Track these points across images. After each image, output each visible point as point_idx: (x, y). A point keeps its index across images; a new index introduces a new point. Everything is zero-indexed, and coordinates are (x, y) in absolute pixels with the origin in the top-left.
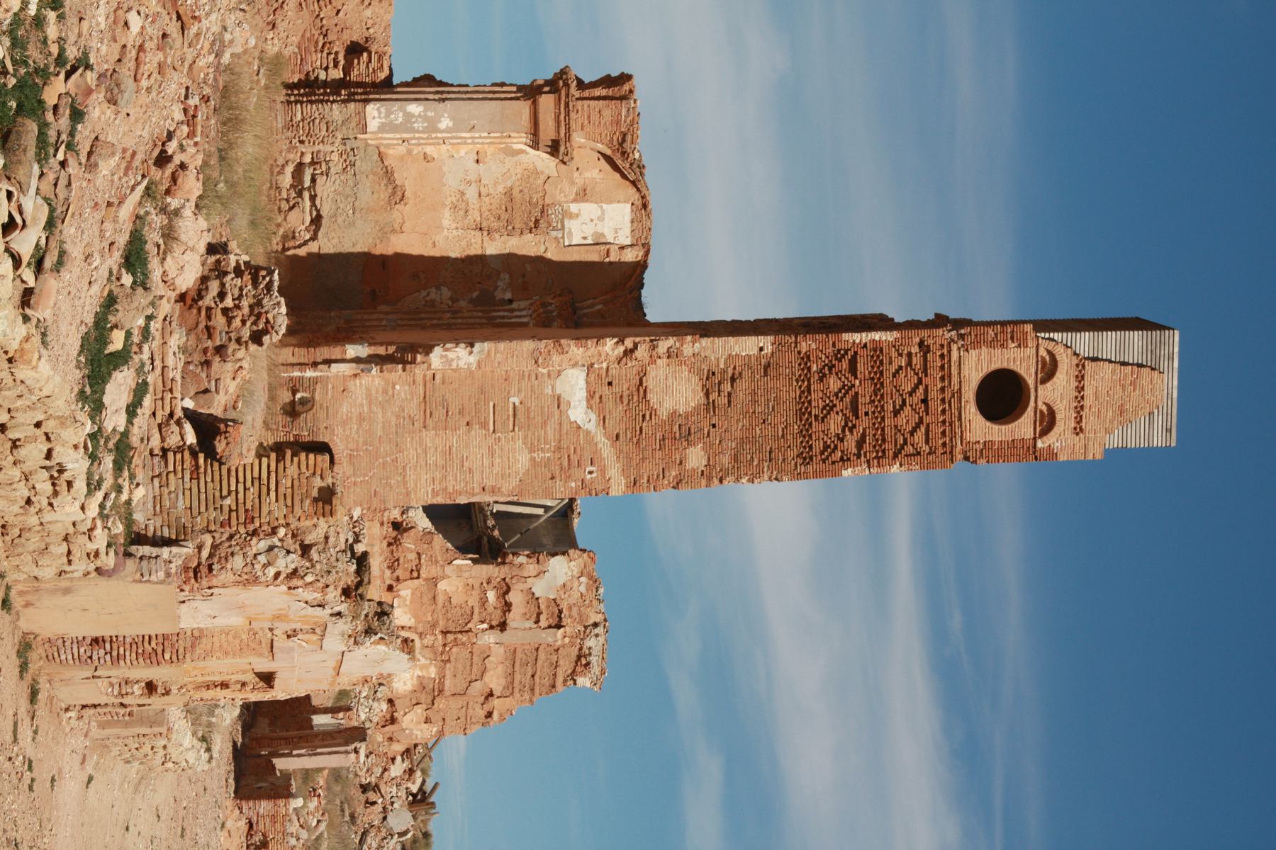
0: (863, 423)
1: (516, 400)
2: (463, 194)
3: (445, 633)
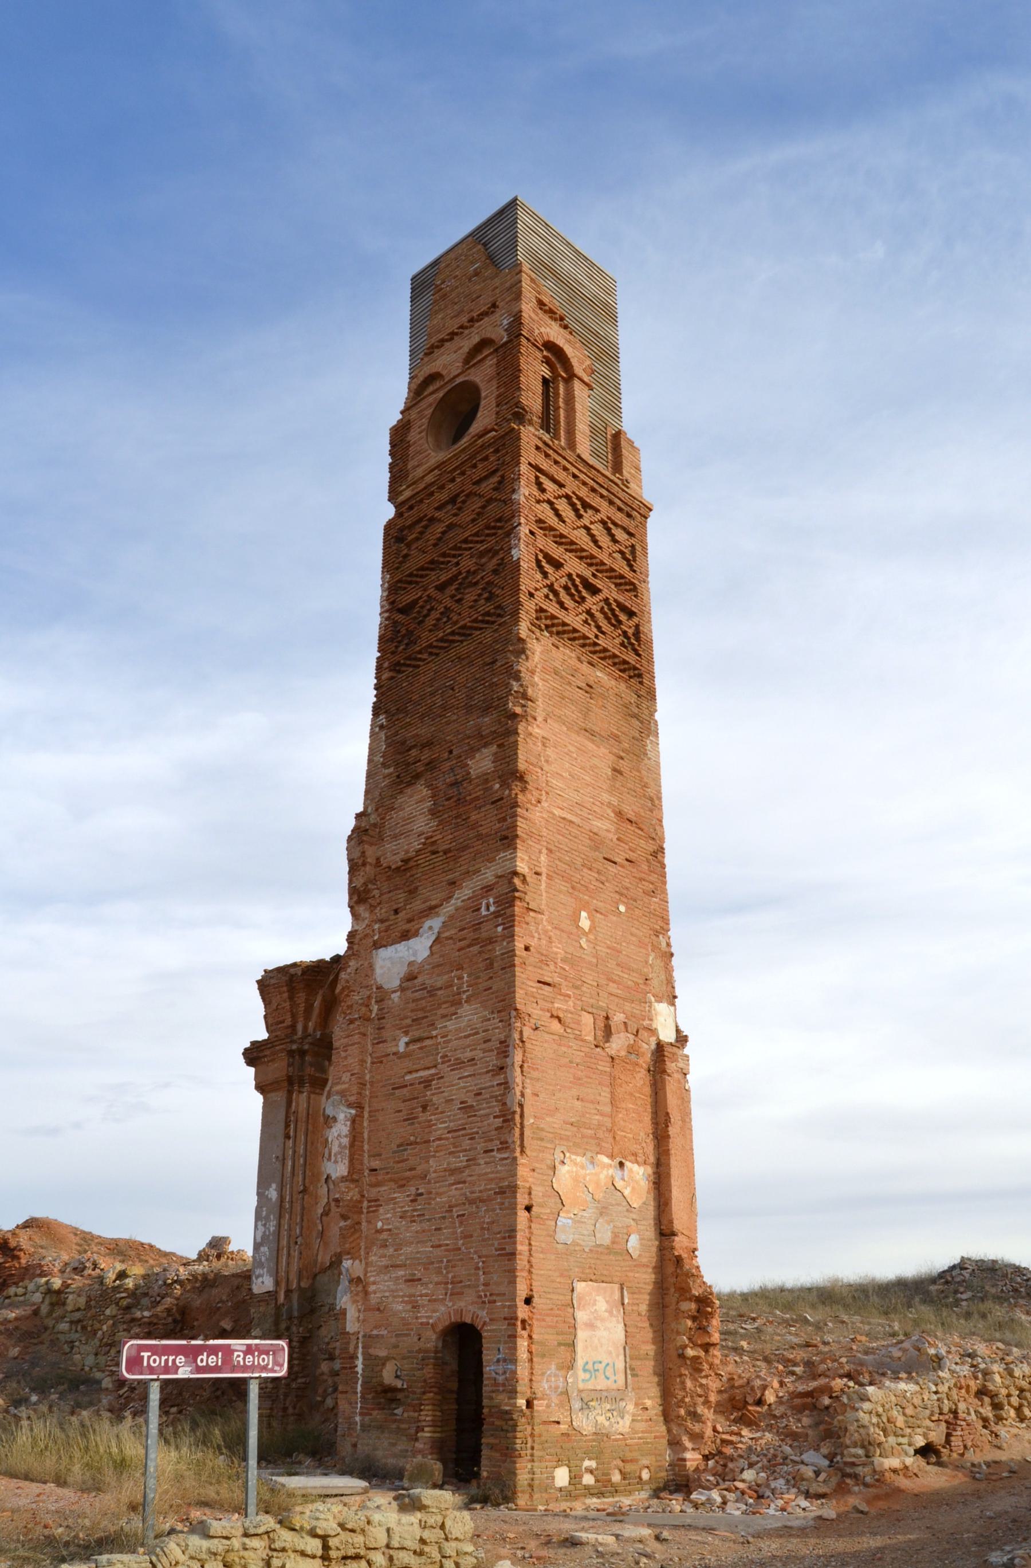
0: (468, 563)
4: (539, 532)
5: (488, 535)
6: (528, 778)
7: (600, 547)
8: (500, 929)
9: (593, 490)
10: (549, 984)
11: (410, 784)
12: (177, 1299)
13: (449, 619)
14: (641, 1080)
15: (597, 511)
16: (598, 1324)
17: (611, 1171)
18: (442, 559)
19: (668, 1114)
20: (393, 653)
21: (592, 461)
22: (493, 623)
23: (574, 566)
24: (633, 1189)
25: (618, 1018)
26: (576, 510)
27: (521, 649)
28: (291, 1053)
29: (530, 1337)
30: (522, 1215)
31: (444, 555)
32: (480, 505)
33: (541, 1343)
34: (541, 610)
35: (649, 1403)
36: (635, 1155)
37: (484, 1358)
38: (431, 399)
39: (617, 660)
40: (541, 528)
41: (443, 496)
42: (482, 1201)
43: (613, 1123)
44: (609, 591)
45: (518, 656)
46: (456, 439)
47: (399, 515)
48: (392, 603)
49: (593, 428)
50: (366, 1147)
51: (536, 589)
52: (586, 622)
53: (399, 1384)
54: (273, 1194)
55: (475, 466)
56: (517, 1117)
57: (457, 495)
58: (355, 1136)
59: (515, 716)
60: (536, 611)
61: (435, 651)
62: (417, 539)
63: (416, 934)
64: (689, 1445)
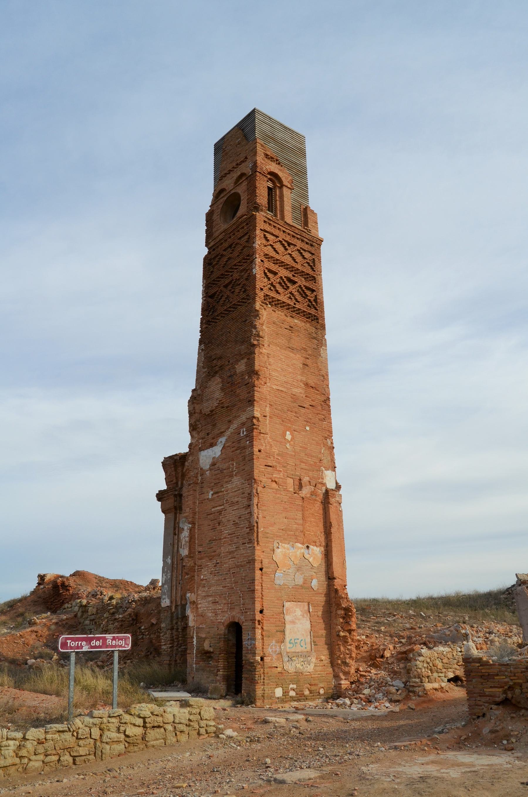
0: (236, 275)
4: (265, 260)
5: (244, 263)
6: (260, 373)
7: (297, 262)
8: (248, 442)
9: (293, 236)
10: (271, 466)
12: (134, 609)
13: (229, 301)
14: (318, 507)
15: (295, 246)
16: (297, 621)
17: (302, 550)
18: (226, 273)
19: (331, 522)
20: (207, 316)
21: (292, 224)
22: (246, 302)
23: (283, 273)
24: (314, 558)
25: (306, 479)
26: (285, 247)
27: (257, 314)
29: (262, 628)
30: (258, 573)
31: (227, 271)
32: (240, 249)
33: (268, 631)
34: (267, 295)
35: (323, 658)
36: (315, 542)
37: (243, 638)
38: (222, 200)
39: (305, 313)
40: (266, 258)
41: (226, 245)
42: (242, 566)
43: (304, 528)
44: (301, 281)
45: (255, 318)
46: (233, 217)
47: (209, 253)
48: (207, 293)
49: (294, 208)
50: (197, 542)
51: (264, 286)
52: (290, 298)
53: (211, 650)
54: (169, 561)
55: (239, 231)
56: (255, 528)
57: (232, 245)
58: (192, 537)
59: (254, 345)
60: (264, 296)
61: (223, 315)
62: (217, 264)
63: (216, 445)
64: (343, 677)
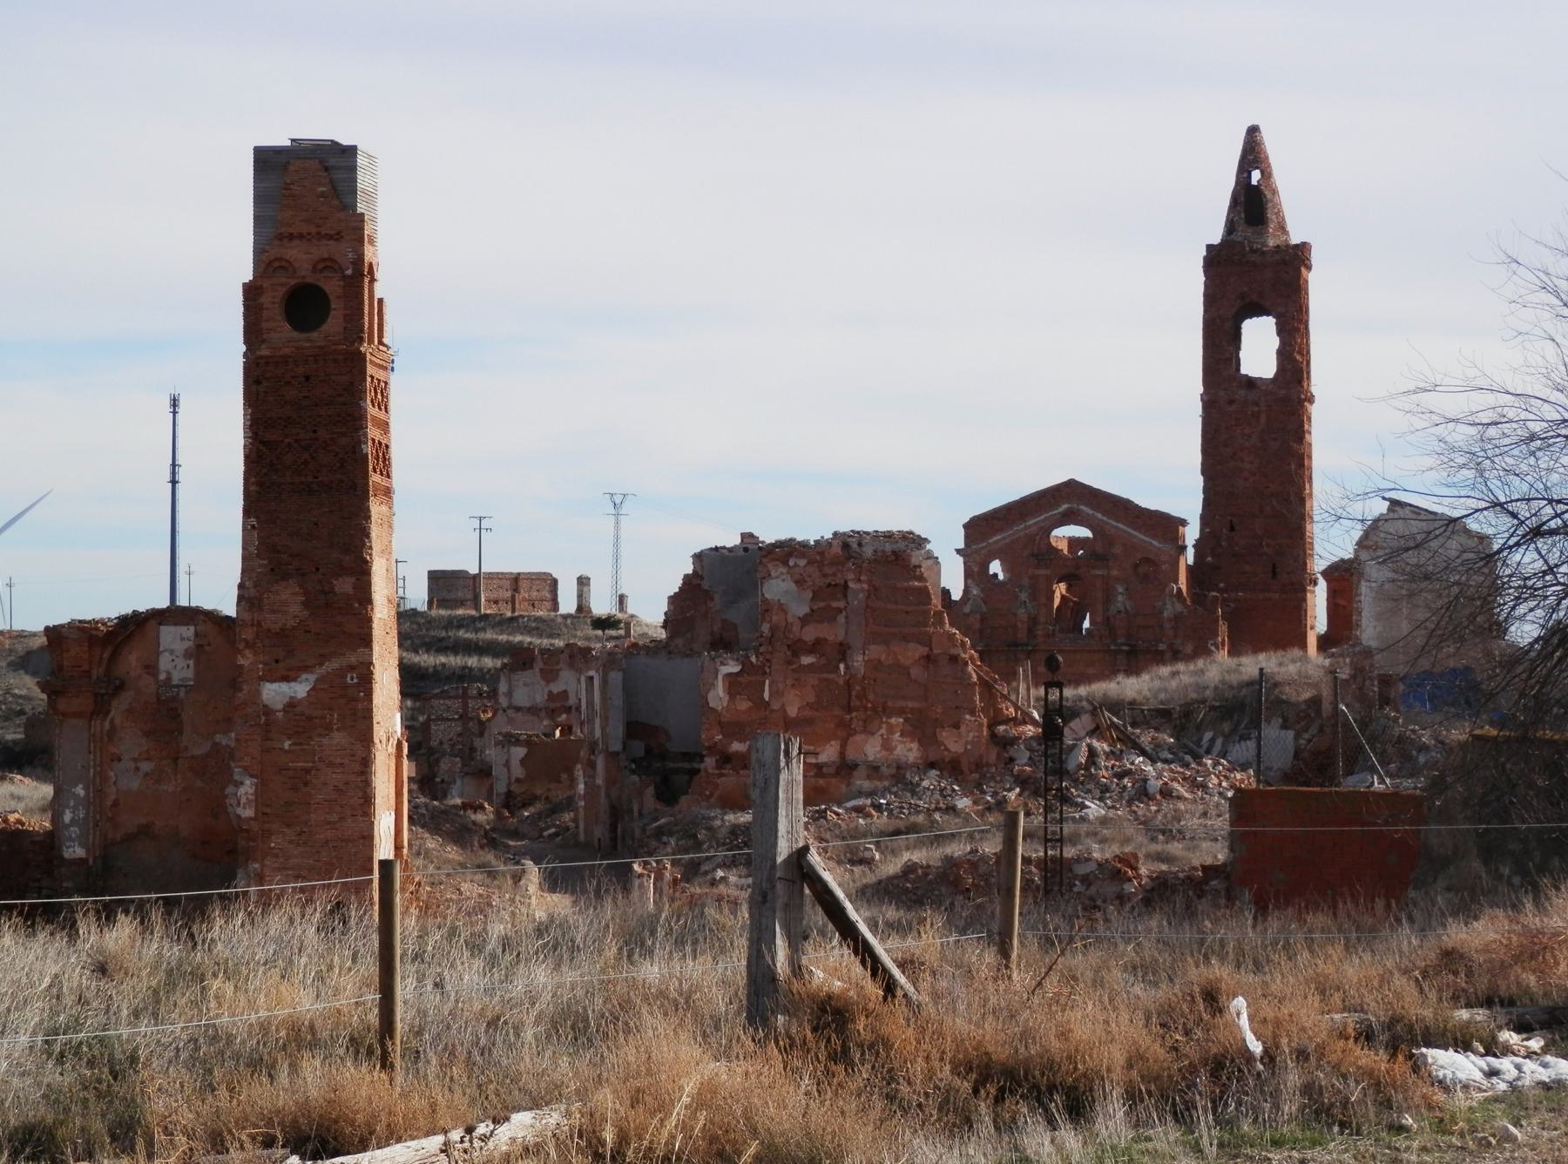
1: (287, 745)
2: (147, 775)
3: (849, 710)
11: (282, 579)
28: (96, 695)
